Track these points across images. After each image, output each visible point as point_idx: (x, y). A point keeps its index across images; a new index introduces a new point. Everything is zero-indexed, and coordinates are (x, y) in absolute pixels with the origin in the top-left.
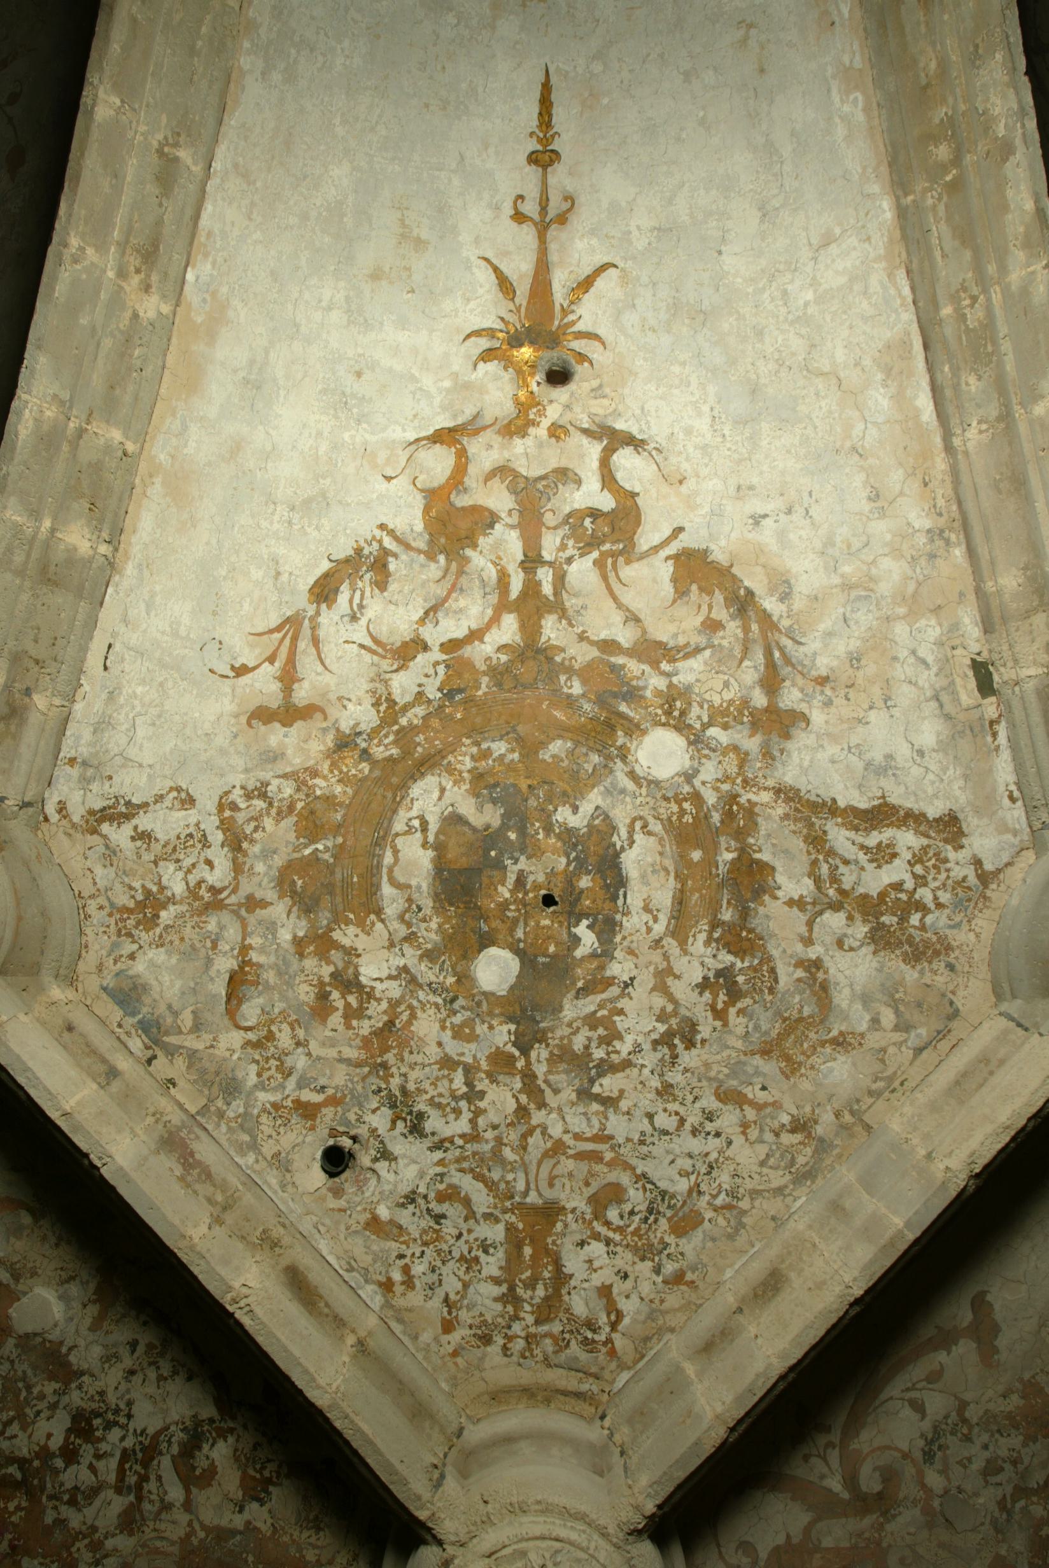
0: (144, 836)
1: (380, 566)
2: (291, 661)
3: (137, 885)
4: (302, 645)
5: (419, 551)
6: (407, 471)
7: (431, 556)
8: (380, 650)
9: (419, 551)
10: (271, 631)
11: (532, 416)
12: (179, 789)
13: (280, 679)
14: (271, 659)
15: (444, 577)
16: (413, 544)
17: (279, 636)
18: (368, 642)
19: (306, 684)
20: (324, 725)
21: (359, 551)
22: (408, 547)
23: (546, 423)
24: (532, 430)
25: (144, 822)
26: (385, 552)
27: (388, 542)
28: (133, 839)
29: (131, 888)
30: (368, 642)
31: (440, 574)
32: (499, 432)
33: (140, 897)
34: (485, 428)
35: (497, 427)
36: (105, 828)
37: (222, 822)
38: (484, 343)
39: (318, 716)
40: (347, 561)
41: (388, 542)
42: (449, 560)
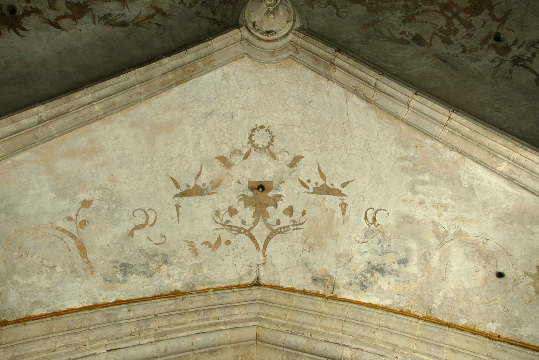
0: (214, 13)
1: (105, 17)
2: (147, 18)
3: (225, 7)
4: (140, 20)
5: (92, 12)
6: (74, 28)
7: (91, 10)
8: (125, 4)
9: (92, 12)
10: (144, 27)
11: (30, 9)
12: (197, 16)
13: (153, 18)
14: (150, 22)
15: (93, 4)
16: (92, 15)
17: (143, 25)
18: (126, 7)
19: (149, 13)
20: (154, 3)
21: (105, 24)
22: (94, 15)
23: (28, 5)
24: (34, 7)
25: (211, 16)
26: (100, 19)
27: (97, 20)
28: (216, 14)
29: (227, 7)
30: (126, 7)
31: (93, 5)
32: (42, 14)
33: (227, 4)
34: (45, 18)
35: (42, 16)
36: (219, 20)
37: (196, 4)
38: (21, 32)
39: (153, 5)
40: (111, 25)
41: (97, 20)
42: (88, 5)
